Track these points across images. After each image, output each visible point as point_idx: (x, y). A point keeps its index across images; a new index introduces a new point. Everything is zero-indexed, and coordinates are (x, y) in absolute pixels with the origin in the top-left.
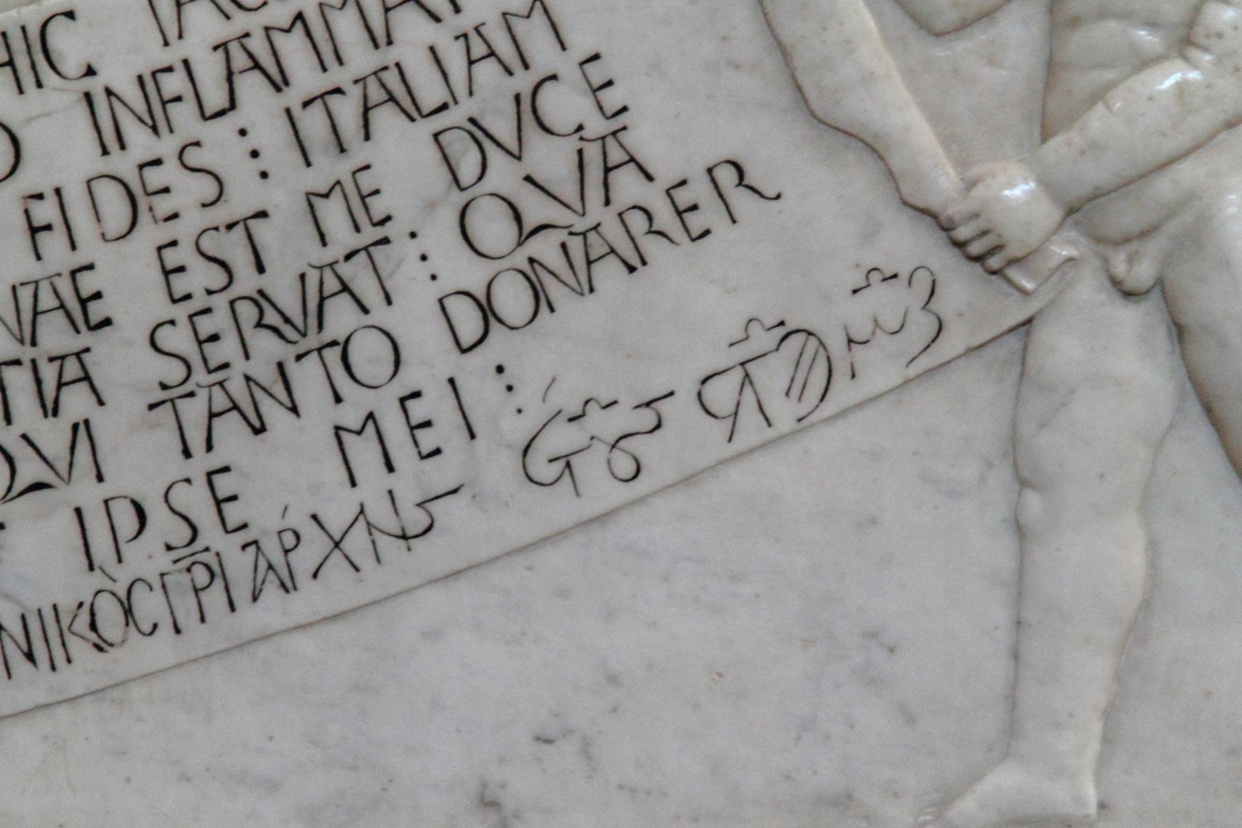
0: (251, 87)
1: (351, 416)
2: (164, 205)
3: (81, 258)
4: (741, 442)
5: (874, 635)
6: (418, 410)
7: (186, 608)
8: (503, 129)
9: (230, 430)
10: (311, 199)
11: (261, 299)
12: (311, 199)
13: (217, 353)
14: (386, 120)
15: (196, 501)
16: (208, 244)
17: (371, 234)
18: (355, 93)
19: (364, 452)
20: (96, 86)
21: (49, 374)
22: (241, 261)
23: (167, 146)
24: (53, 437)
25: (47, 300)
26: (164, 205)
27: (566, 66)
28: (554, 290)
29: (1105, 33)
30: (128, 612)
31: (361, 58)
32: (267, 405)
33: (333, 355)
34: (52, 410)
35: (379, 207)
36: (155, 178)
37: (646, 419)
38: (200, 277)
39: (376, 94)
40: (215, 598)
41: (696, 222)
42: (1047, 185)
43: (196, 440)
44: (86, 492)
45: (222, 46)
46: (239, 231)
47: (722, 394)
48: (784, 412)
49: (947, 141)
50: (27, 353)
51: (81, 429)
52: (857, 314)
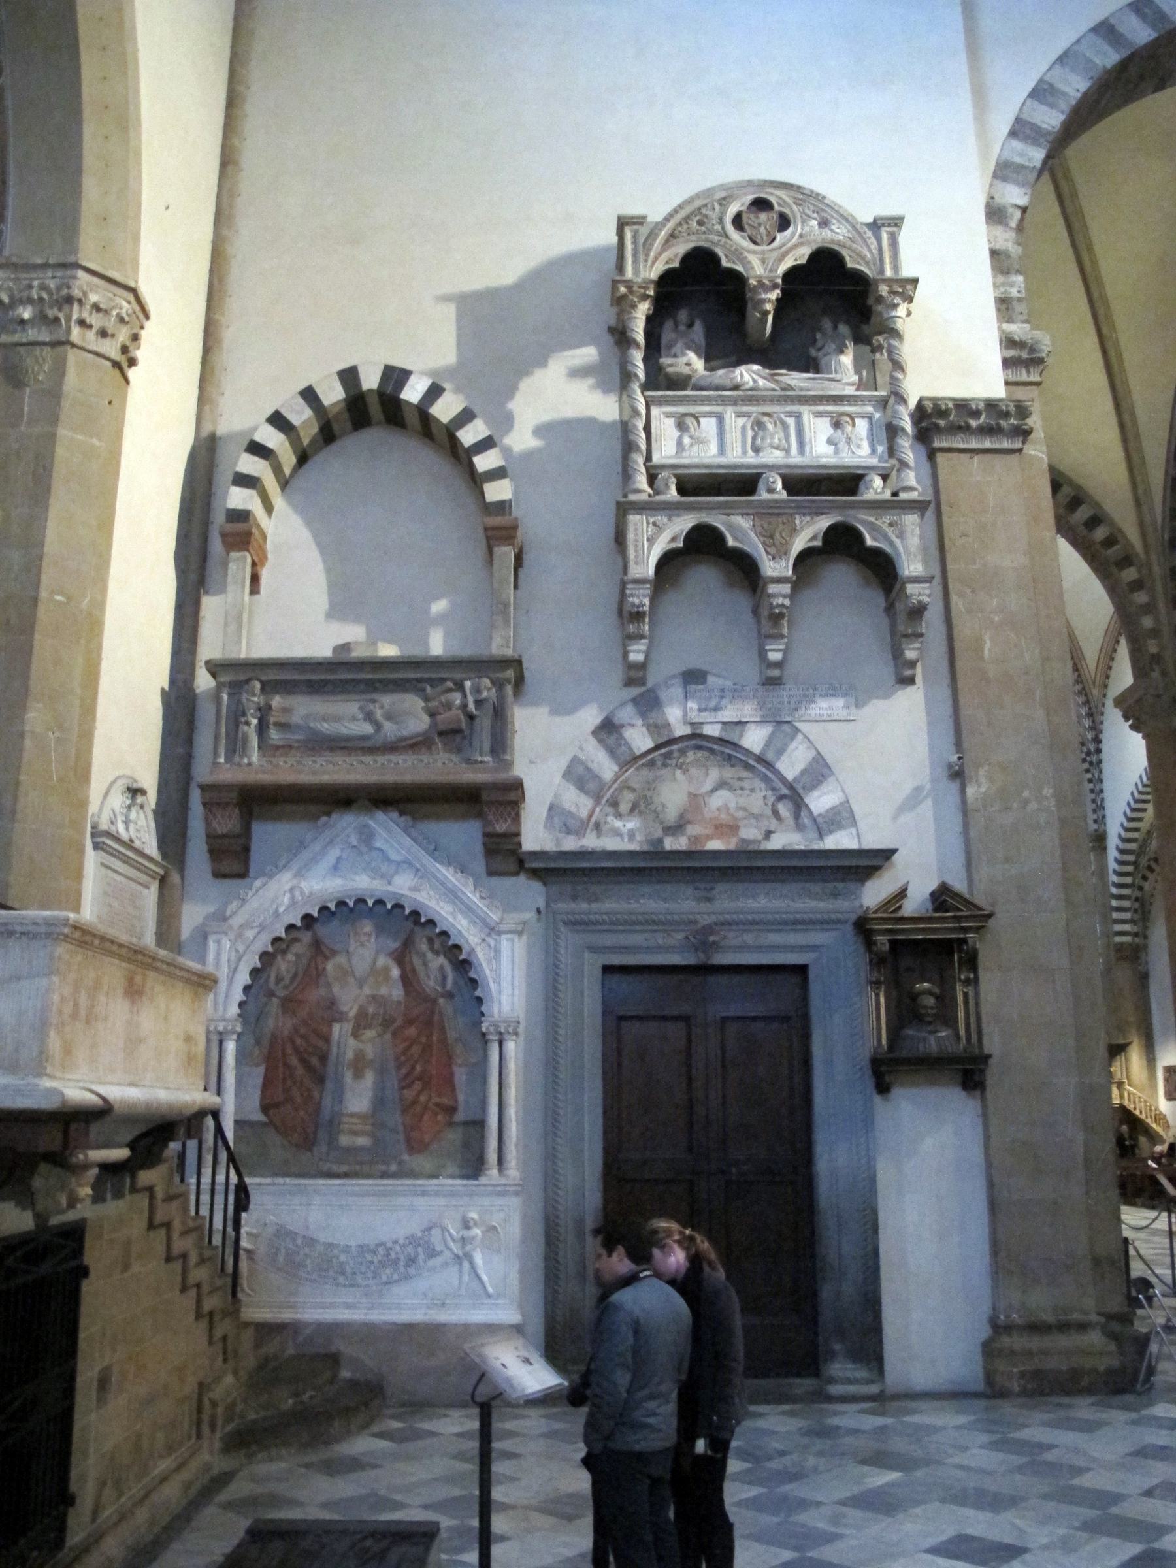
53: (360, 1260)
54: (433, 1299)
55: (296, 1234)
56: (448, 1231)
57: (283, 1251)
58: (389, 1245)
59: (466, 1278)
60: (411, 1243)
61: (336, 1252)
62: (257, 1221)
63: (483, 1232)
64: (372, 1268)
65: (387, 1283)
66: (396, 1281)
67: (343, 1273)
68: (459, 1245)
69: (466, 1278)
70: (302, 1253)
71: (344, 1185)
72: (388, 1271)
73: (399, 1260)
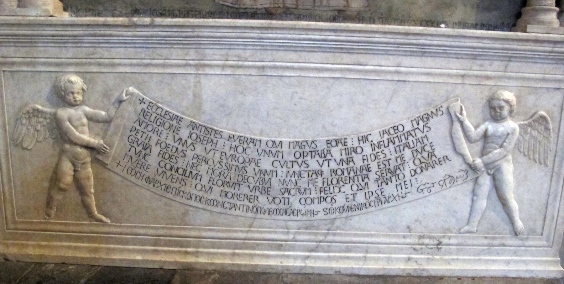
0: (391, 144)
1: (398, 183)
2: (379, 157)
3: (368, 163)
4: (443, 189)
5: (455, 211)
6: (406, 183)
7: (377, 204)
8: (420, 150)
9: (384, 184)
10: (396, 158)
11: (389, 169)
12: (396, 158)
13: (383, 175)
14: (406, 149)
15: (379, 192)
16: (384, 162)
17: (403, 162)
18: (403, 145)
19: (399, 187)
20: (373, 143)
21: (363, 177)
22: (387, 163)
23: (380, 150)
24: (363, 184)
25: (364, 168)
26: (379, 157)
27: (428, 144)
28: (424, 170)
29: (493, 145)
30: (370, 204)
31: (404, 141)
32: (388, 181)
33: (397, 176)
34: (363, 181)
35: (404, 159)
36: (378, 154)
37: (432, 185)
38: (382, 166)
39: (405, 146)
40: (380, 203)
41: (441, 163)
42: (483, 162)
43: (380, 185)
44: (366, 191)
45: (388, 139)
46: (387, 161)
47: (441, 183)
48: (448, 185)
49: (471, 155)
50: (361, 174)
51: (366, 183)
52: (458, 175)
53: (296, 168)
54: (421, 237)
55: (179, 119)
56: (462, 123)
57: (156, 150)
58: (352, 143)
59: (482, 203)
60: (391, 141)
61: (252, 152)
62: (106, 95)
63: (521, 126)
64: (320, 184)
65: (342, 209)
66: (359, 207)
67: (266, 191)
68: (478, 147)
69: (482, 203)
70: (189, 153)
71: (267, 28)
72: (347, 189)
73: (368, 169)
